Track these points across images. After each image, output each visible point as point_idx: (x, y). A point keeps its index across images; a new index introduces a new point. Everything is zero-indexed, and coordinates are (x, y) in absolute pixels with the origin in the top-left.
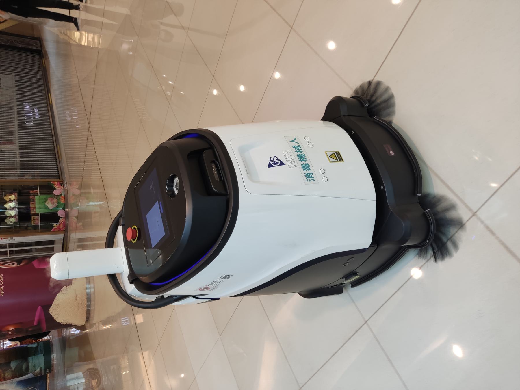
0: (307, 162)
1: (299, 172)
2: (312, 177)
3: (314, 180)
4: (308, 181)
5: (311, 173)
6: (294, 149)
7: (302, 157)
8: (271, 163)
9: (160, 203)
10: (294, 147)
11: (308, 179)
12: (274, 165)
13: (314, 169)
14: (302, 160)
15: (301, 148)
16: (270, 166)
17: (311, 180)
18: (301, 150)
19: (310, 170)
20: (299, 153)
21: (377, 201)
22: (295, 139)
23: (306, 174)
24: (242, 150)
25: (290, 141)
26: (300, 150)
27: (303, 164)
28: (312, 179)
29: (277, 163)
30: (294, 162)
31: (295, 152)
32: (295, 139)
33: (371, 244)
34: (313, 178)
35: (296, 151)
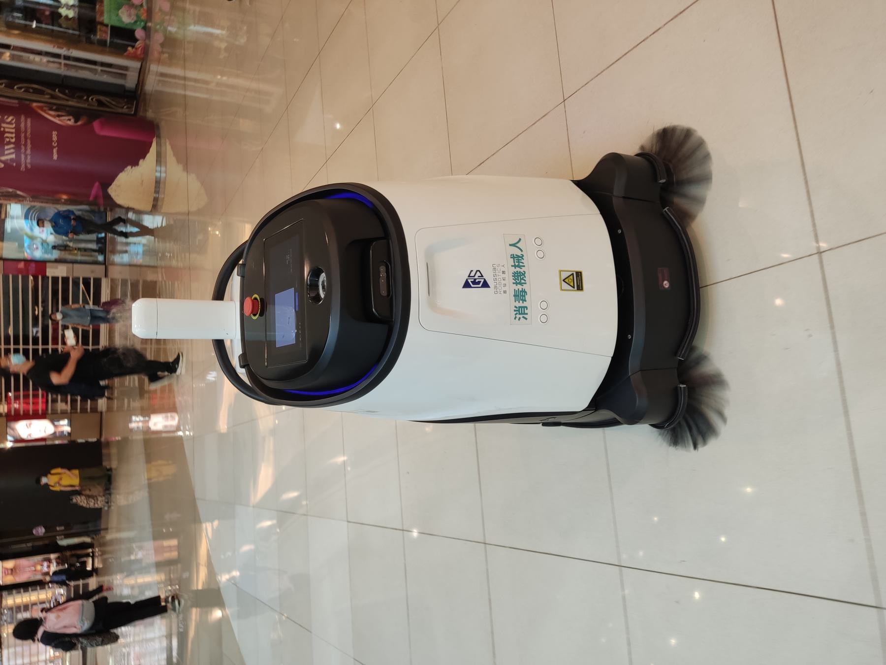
0: (525, 287)
1: (508, 302)
2: (525, 314)
3: (526, 319)
4: (517, 319)
5: (524, 307)
6: (511, 262)
7: (519, 278)
8: (469, 281)
9: (297, 294)
10: (513, 257)
11: (518, 316)
12: (472, 286)
13: (533, 302)
14: (518, 282)
15: (523, 259)
16: (467, 285)
17: (522, 319)
18: (523, 263)
19: (526, 301)
20: (518, 269)
21: (613, 358)
22: (520, 239)
23: (517, 308)
24: (430, 254)
25: (510, 245)
26: (521, 264)
27: (518, 289)
28: (523, 317)
29: (479, 283)
30: (505, 285)
31: (512, 266)
32: (520, 239)
33: (587, 408)
34: (525, 316)
35: (513, 264)
